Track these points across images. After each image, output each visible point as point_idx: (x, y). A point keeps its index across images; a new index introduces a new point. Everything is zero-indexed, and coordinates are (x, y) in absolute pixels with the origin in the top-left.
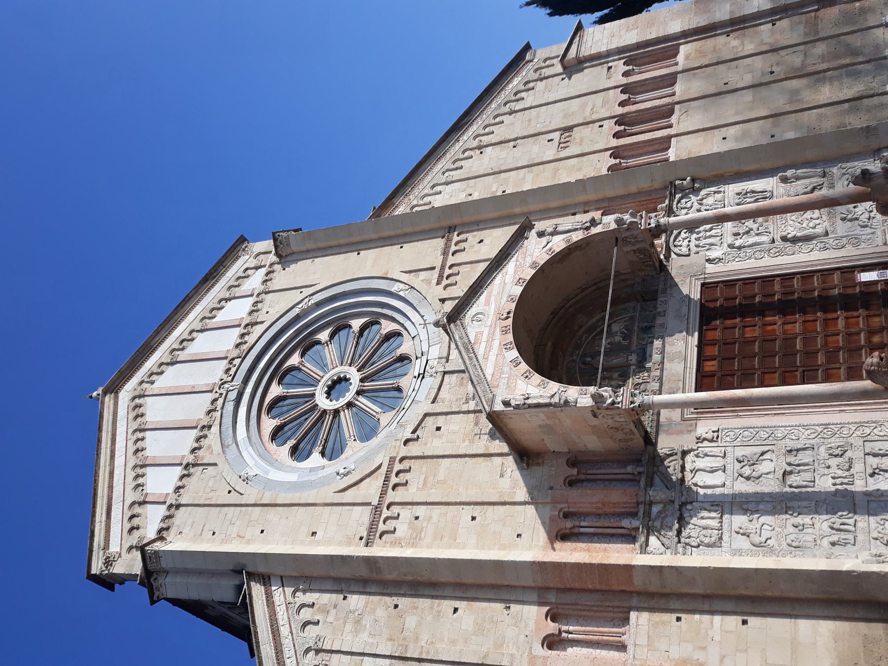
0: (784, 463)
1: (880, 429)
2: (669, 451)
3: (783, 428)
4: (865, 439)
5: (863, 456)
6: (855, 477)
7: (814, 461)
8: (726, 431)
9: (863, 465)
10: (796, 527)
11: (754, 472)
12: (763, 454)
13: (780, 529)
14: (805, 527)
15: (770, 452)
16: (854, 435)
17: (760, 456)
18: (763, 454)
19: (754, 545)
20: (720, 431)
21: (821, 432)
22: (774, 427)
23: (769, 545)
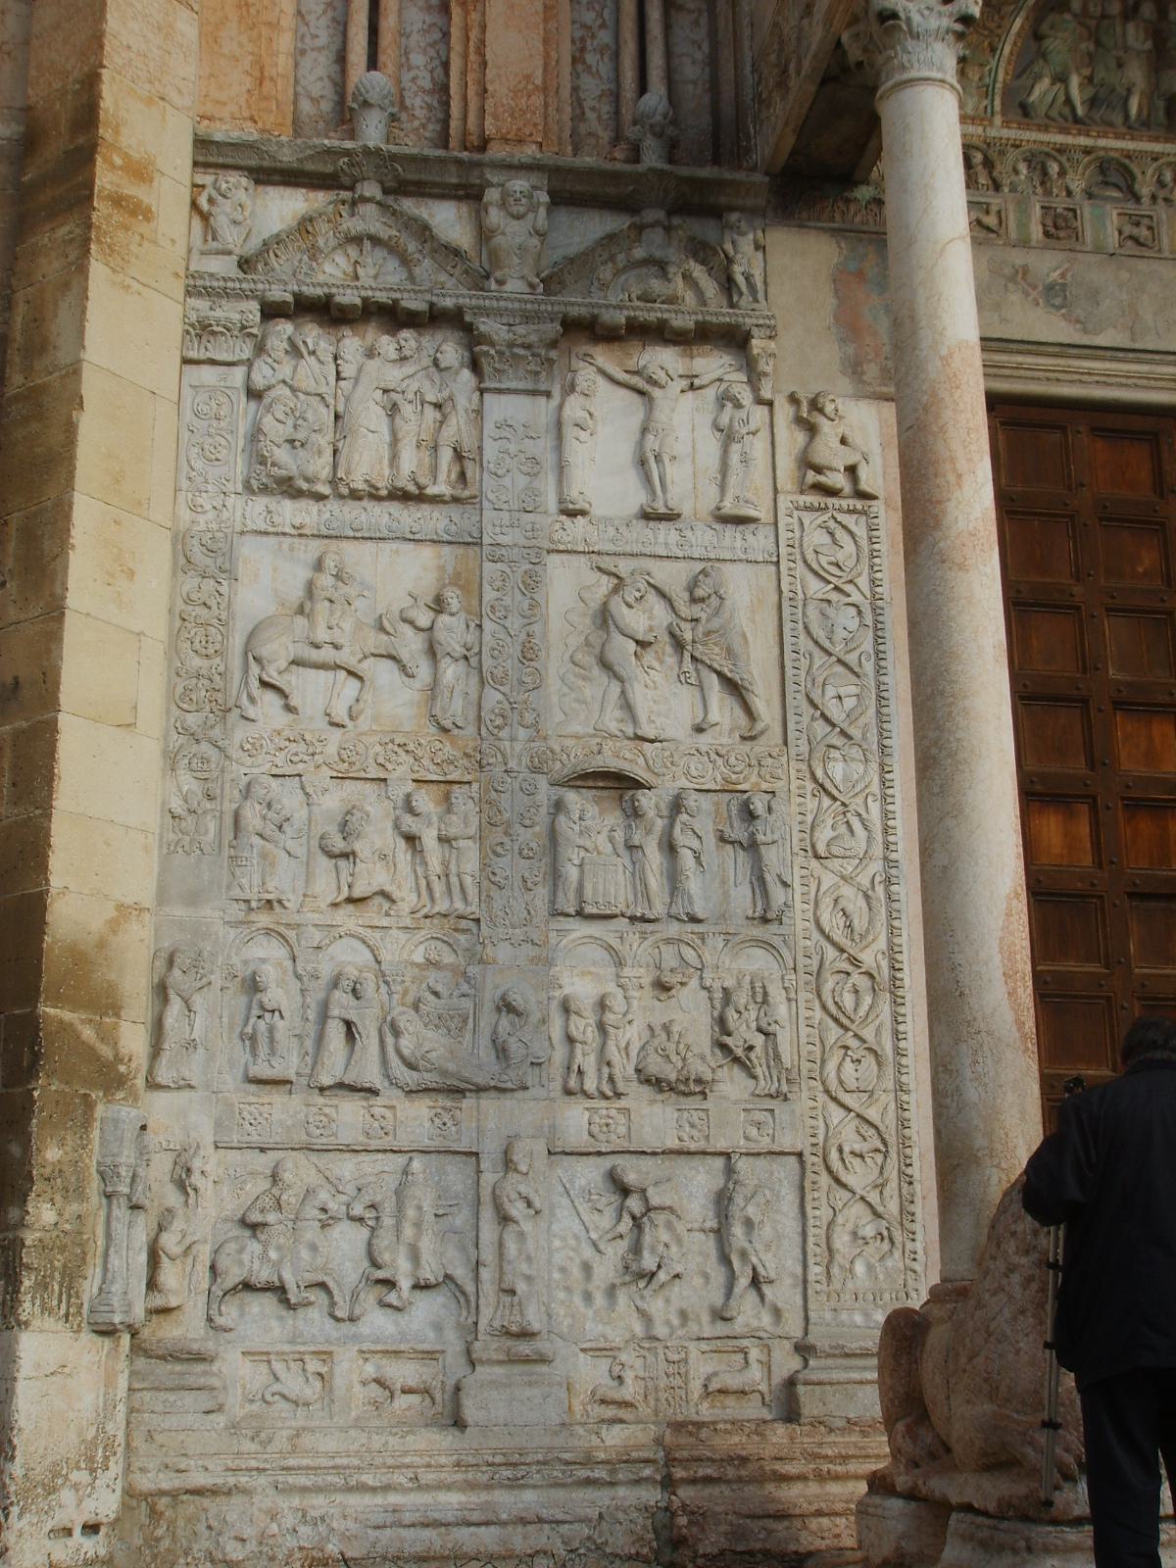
0: (684, 783)
1: (869, 1231)
2: (748, 278)
3: (875, 787)
4: (809, 1159)
5: (722, 1145)
6: (604, 1103)
7: (694, 920)
8: (861, 531)
9: (672, 1143)
10: (344, 826)
11: (632, 646)
12: (734, 687)
13: (332, 749)
14: (342, 863)
15: (742, 719)
16: (836, 1114)
17: (719, 674)
18: (734, 687)
19: (251, 636)
20: (859, 504)
21: (855, 962)
22: (883, 747)
23: (252, 700)
